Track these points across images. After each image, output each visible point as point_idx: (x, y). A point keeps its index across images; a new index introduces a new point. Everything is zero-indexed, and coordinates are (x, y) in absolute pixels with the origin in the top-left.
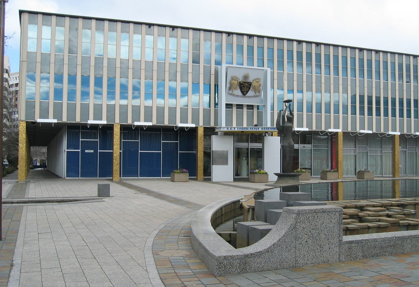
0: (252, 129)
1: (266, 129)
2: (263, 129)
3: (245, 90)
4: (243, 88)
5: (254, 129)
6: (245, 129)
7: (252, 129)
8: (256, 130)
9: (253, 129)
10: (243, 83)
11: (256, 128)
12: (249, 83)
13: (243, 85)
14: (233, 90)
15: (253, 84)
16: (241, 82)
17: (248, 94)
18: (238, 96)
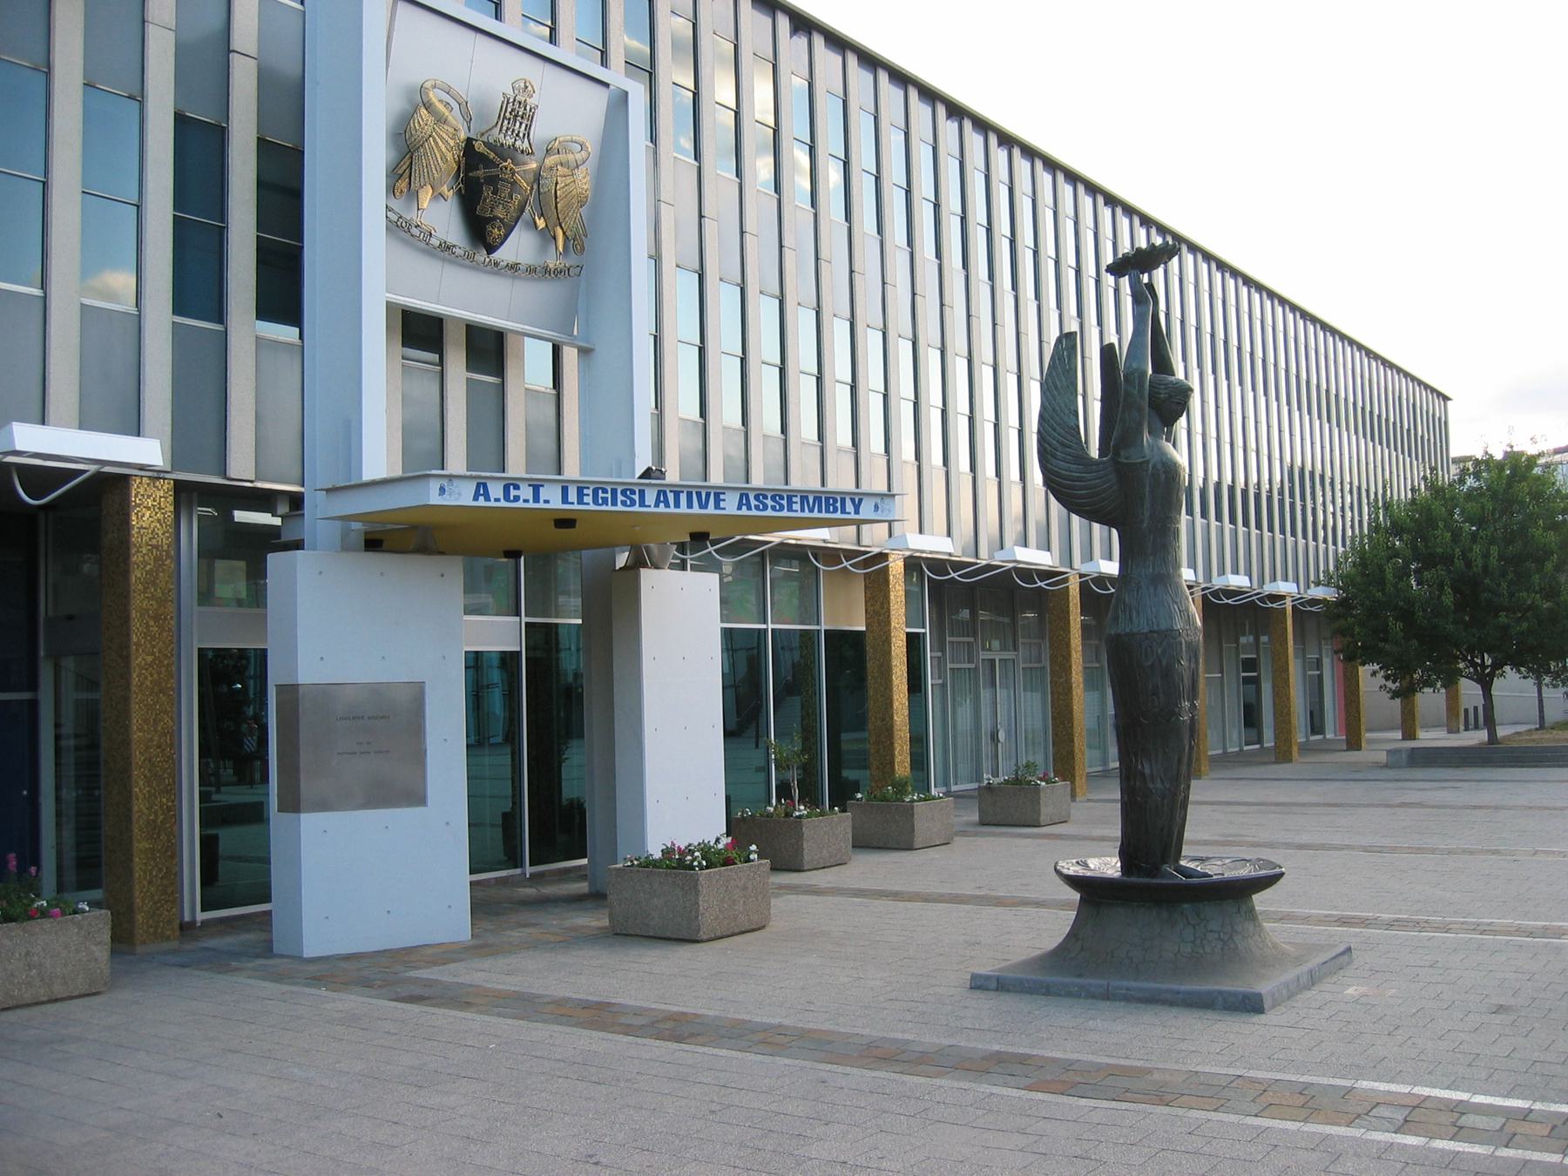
0: (671, 497)
1: (769, 502)
2: (753, 502)
4: (487, 192)
5: (690, 505)
6: (620, 498)
7: (671, 497)
8: (701, 506)
9: (677, 505)
10: (492, 155)
11: (699, 495)
13: (494, 171)
16: (479, 147)
18: (446, 247)
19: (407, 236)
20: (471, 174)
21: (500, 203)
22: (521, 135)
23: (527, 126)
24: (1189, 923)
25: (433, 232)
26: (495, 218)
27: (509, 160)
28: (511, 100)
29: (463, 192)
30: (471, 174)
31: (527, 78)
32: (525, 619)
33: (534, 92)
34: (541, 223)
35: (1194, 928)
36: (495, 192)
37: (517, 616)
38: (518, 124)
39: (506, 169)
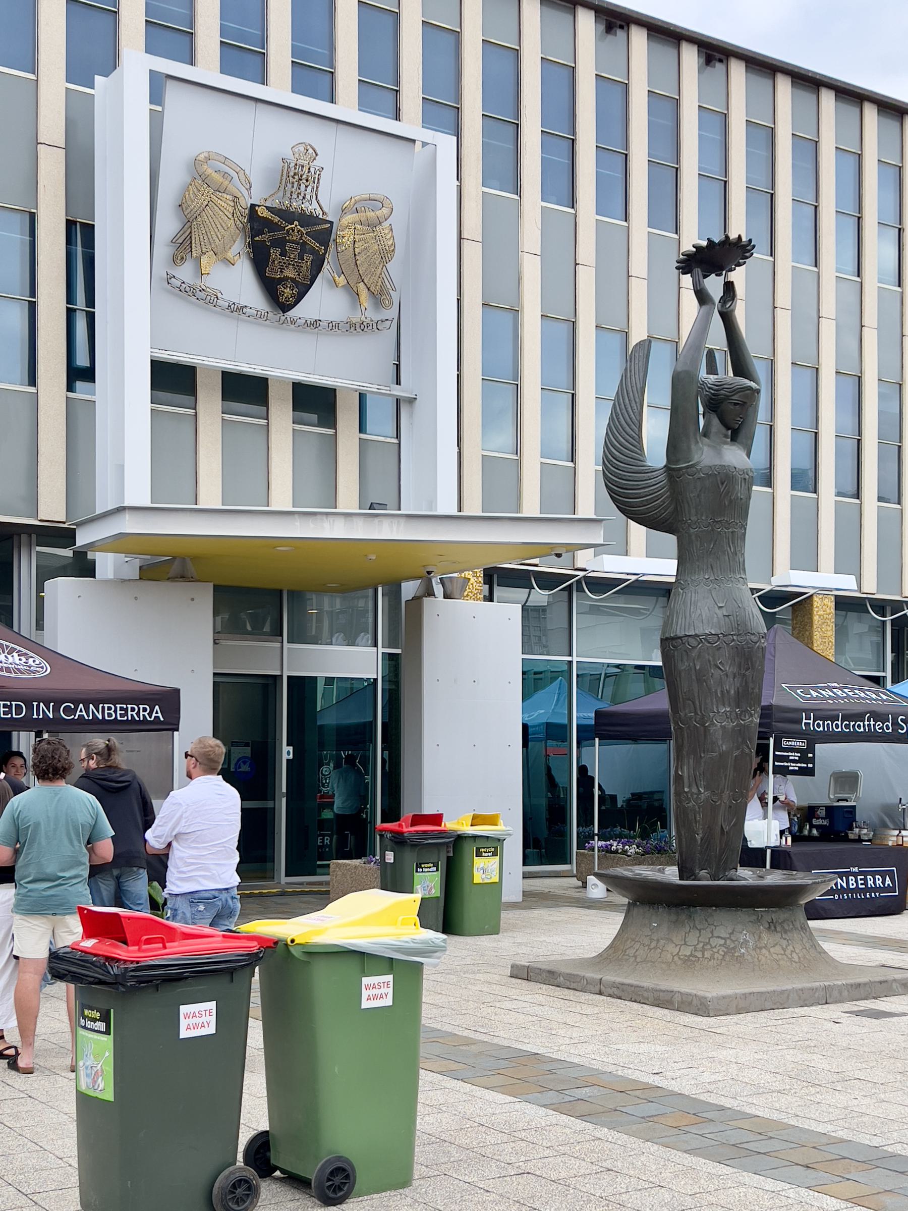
3: (290, 273)
4: (275, 253)
10: (276, 219)
12: (308, 220)
13: (279, 234)
14: (204, 259)
15: (345, 237)
16: (263, 212)
17: (306, 309)
18: (236, 309)
19: (193, 299)
20: (257, 238)
21: (289, 264)
22: (308, 197)
23: (313, 188)
24: (695, 926)
25: (219, 295)
26: (286, 279)
27: (296, 223)
28: (292, 165)
29: (252, 256)
30: (257, 238)
31: (307, 142)
32: (381, 650)
33: (317, 155)
34: (341, 280)
35: (700, 932)
36: (283, 254)
37: (375, 647)
38: (303, 187)
39: (293, 231)
